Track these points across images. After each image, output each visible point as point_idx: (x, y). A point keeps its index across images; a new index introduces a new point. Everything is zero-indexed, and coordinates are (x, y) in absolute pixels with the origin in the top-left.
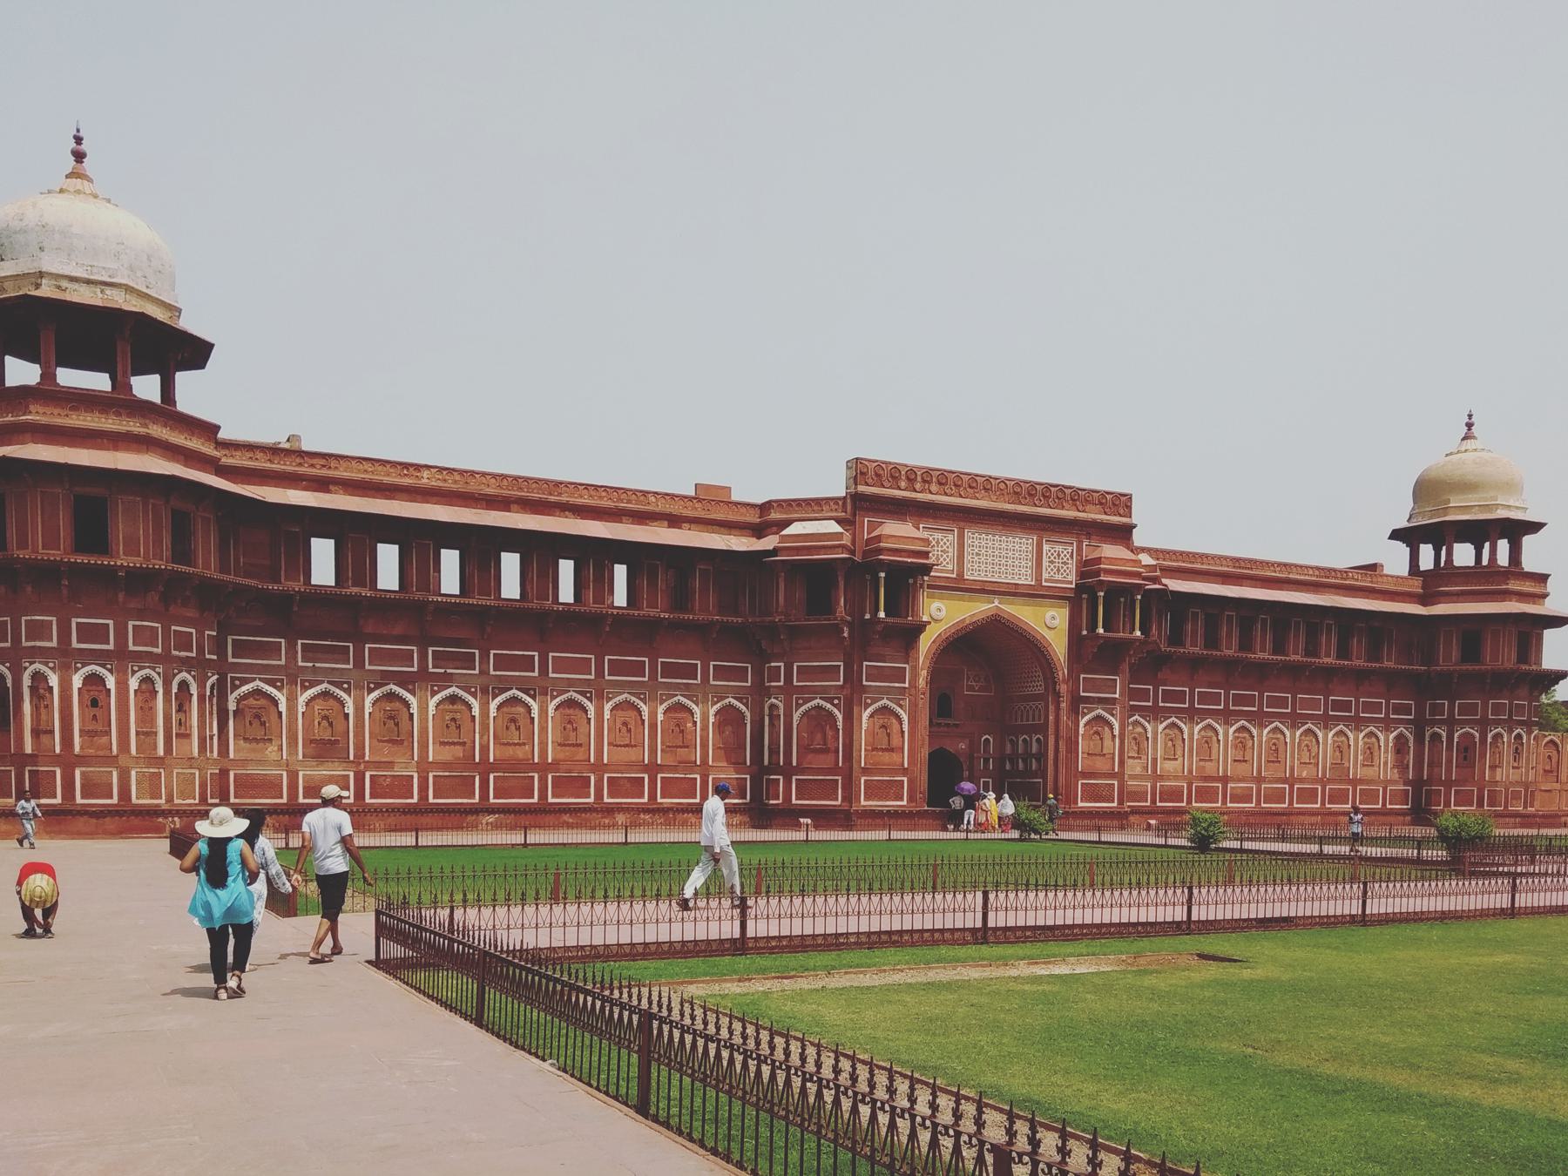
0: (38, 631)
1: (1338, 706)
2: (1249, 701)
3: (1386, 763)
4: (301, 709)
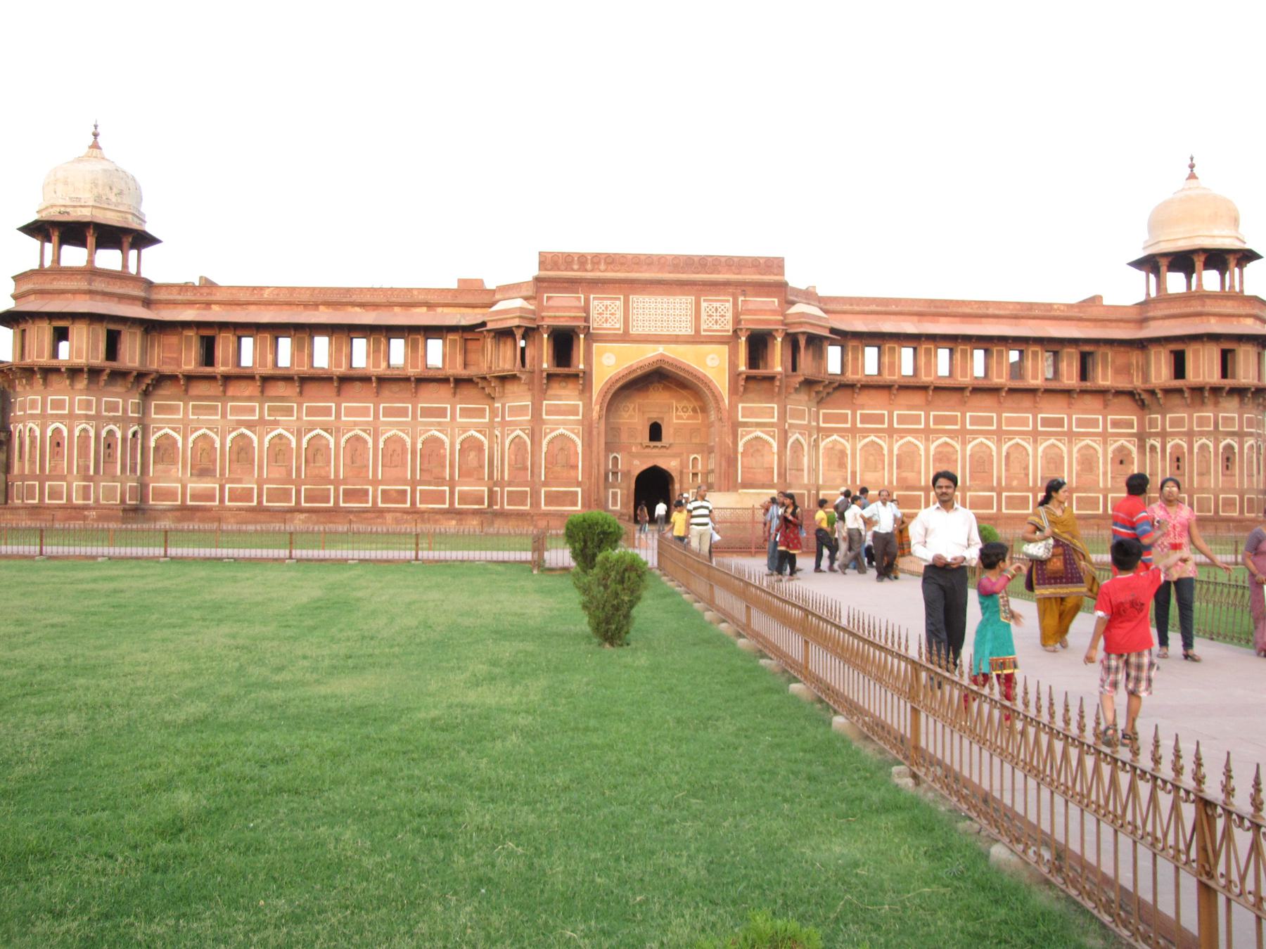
0: (33, 404)
1: (1046, 422)
2: (953, 420)
4: (190, 445)
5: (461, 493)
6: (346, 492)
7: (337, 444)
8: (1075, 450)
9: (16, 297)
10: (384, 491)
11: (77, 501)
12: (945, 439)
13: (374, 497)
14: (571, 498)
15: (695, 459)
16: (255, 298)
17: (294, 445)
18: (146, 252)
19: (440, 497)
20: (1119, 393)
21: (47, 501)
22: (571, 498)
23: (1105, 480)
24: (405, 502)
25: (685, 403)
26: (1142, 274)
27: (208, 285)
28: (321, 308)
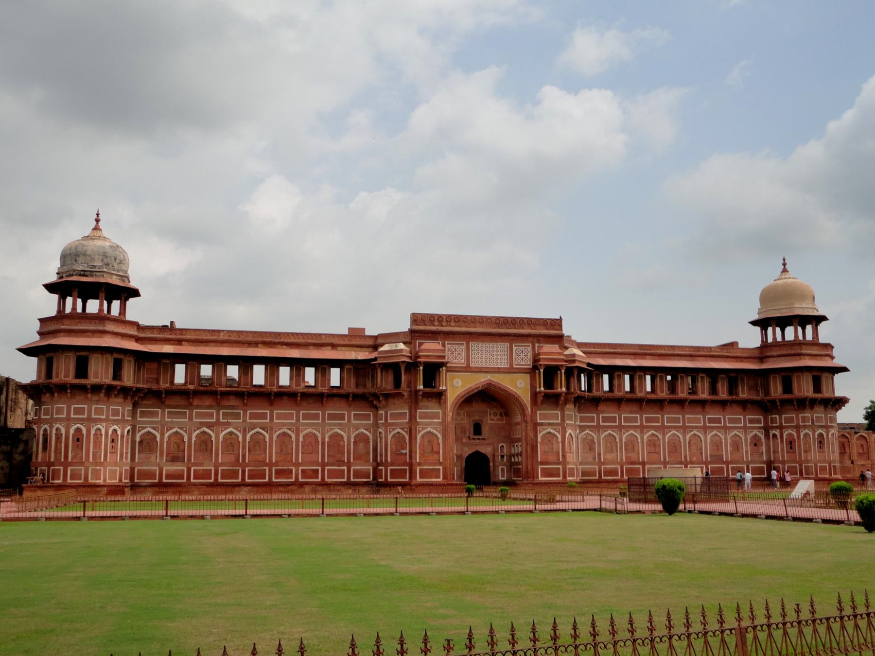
2: (656, 420)
3: (747, 452)
4: (166, 440)
5: (354, 470)
6: (277, 472)
7: (271, 438)
8: (729, 437)
9: (40, 333)
10: (303, 471)
11: (91, 481)
12: (652, 432)
13: (297, 473)
14: (435, 473)
15: (502, 446)
16: (214, 338)
17: (240, 439)
18: (131, 302)
19: (340, 474)
20: (753, 403)
21: (69, 481)
22: (435, 473)
23: (747, 457)
24: (317, 478)
25: (495, 410)
26: (758, 329)
27: (171, 328)
28: (260, 345)
